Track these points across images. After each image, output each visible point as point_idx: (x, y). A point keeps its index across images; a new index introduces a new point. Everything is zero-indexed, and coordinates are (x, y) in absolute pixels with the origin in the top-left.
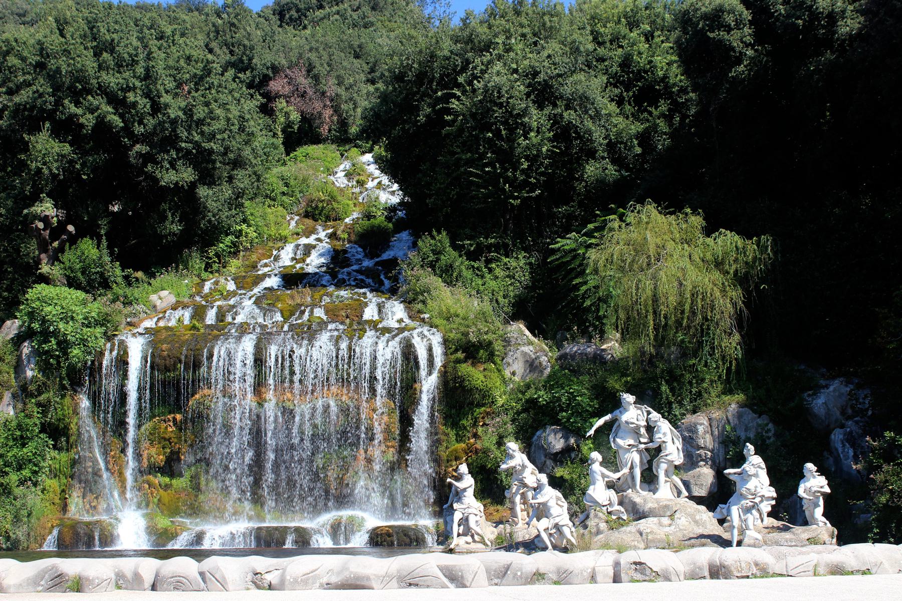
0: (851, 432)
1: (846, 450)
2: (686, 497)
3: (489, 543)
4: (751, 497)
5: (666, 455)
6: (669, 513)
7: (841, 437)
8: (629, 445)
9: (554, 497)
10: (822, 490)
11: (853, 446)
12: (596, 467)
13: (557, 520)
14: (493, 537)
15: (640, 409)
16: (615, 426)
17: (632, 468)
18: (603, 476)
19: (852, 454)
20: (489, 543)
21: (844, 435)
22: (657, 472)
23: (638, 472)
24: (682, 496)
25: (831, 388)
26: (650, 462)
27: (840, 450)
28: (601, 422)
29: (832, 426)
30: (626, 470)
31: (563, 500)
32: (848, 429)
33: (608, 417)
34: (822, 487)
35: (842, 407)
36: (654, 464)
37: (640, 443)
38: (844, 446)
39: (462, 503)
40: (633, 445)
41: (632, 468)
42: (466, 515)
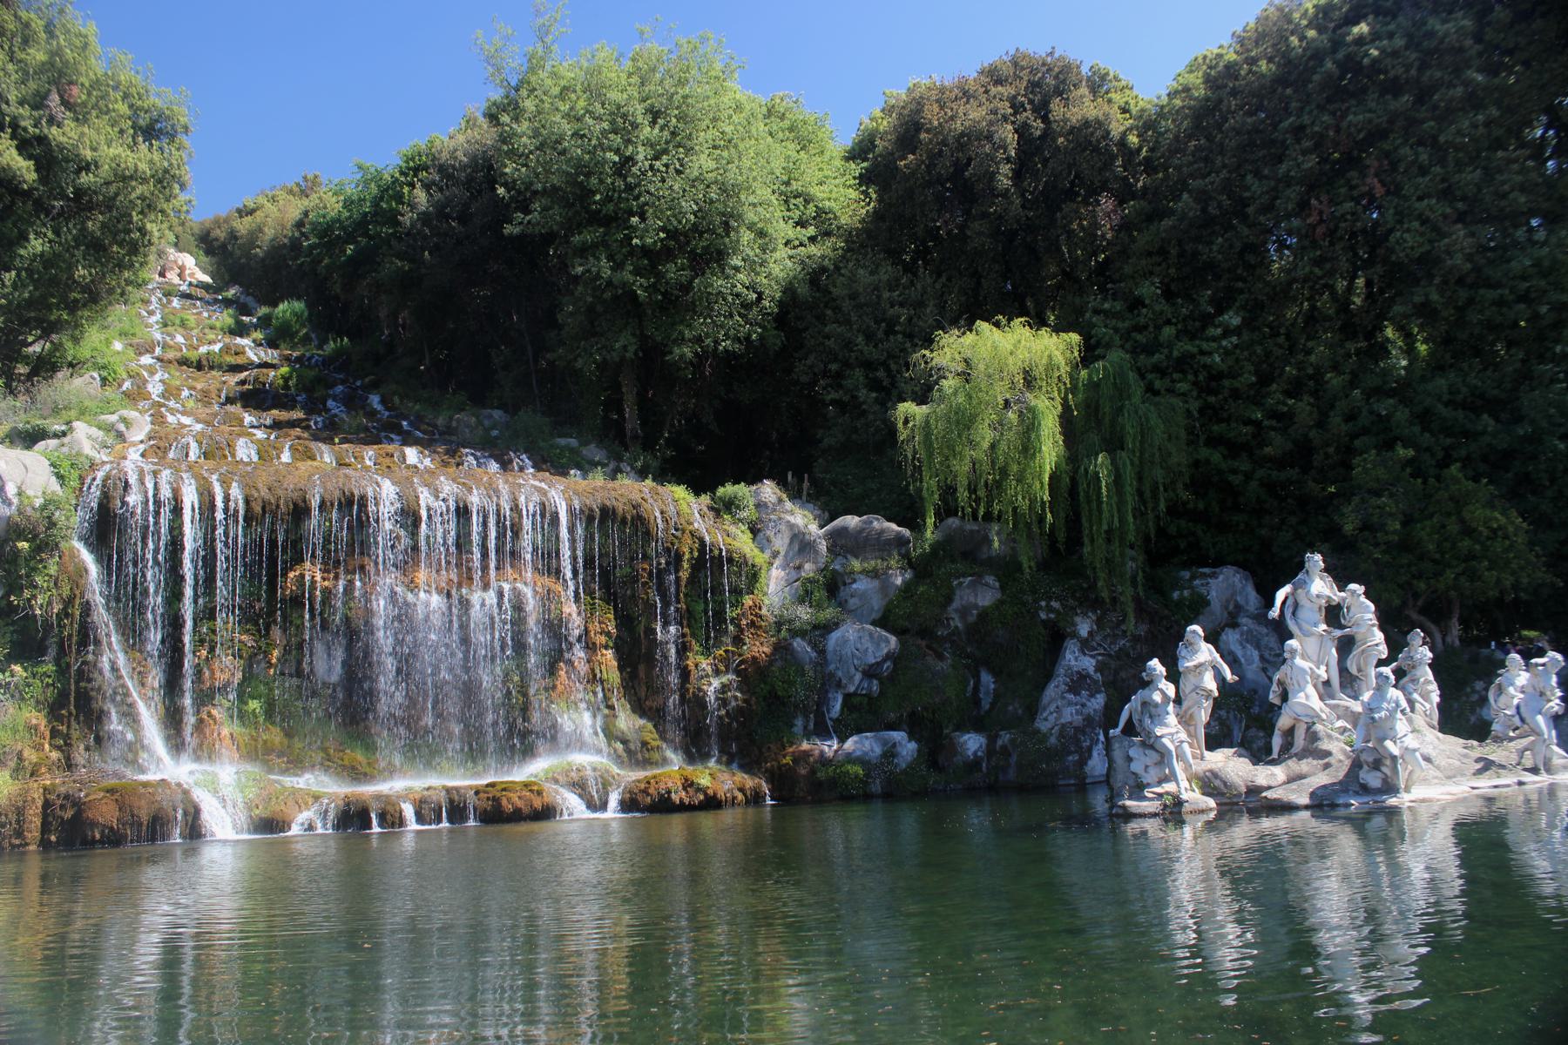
0: (1250, 631)
7: (1237, 636)
11: (1258, 647)
21: (1242, 635)
33: (1287, 589)
39: (1166, 725)
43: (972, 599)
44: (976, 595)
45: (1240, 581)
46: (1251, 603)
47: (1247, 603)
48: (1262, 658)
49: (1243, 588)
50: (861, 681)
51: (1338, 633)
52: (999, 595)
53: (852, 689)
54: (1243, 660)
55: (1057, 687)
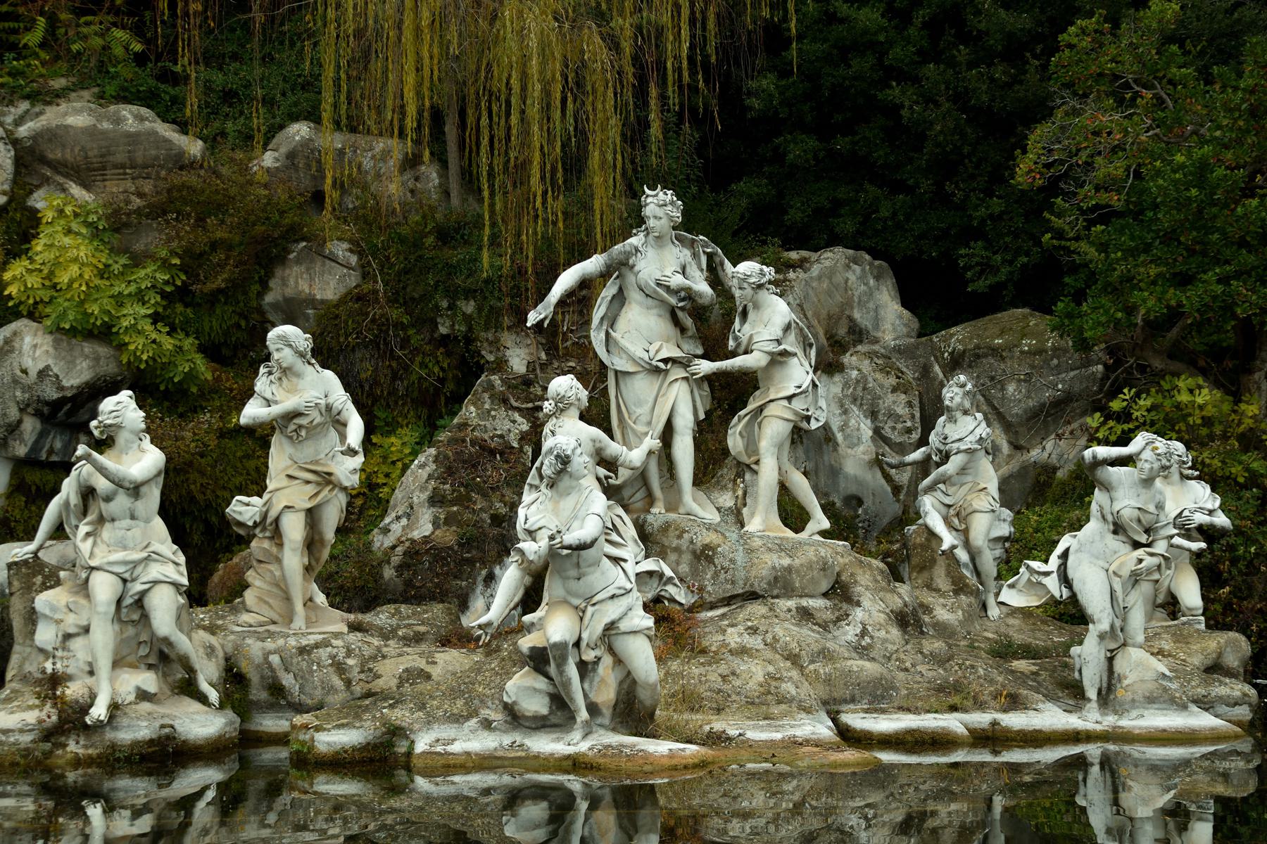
0: (862, 381)
1: (853, 422)
2: (824, 534)
5: (789, 398)
8: (665, 361)
11: (873, 414)
13: (611, 612)
15: (691, 245)
17: (668, 434)
19: (870, 433)
21: (846, 385)
24: (812, 527)
25: (815, 270)
28: (566, 280)
30: (652, 442)
32: (855, 373)
33: (592, 265)
34: (1211, 512)
35: (830, 317)
38: (845, 412)
41: (668, 434)
42: (138, 587)
43: (304, 287)
44: (312, 279)
45: (862, 278)
46: (888, 326)
47: (877, 326)
48: (877, 432)
49: (870, 294)
50: (42, 435)
51: (705, 367)
52: (353, 280)
53: (21, 451)
54: (839, 437)
55: (422, 466)
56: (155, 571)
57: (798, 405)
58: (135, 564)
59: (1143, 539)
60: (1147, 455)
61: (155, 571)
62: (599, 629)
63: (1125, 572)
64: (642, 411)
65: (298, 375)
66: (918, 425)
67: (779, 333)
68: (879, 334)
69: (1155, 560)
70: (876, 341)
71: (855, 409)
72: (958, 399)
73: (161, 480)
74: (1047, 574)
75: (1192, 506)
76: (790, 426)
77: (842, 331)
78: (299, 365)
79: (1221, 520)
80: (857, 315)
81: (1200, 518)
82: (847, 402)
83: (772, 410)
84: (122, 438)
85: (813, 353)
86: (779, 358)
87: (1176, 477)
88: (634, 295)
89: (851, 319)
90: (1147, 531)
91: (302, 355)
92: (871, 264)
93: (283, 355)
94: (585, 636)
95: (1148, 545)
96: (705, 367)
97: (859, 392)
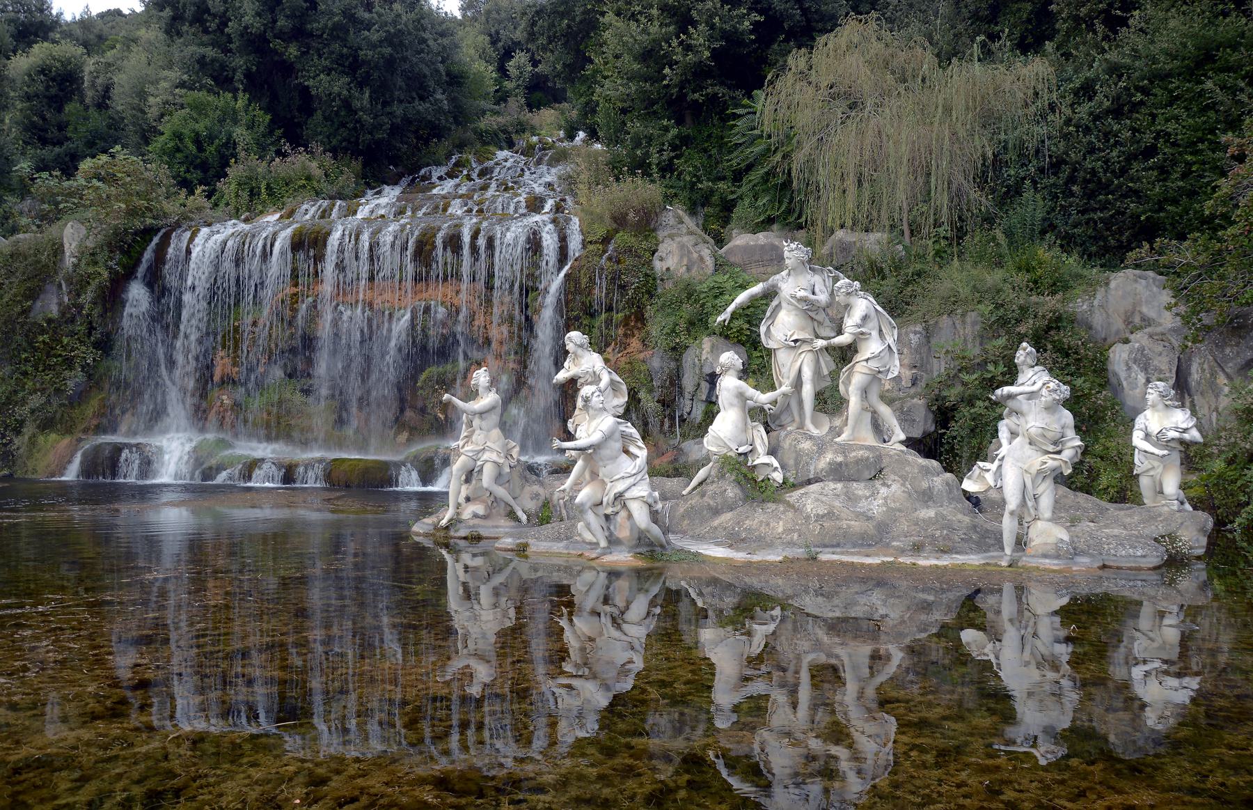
0: (1142, 349)
2: (902, 442)
3: (524, 518)
4: (1051, 448)
5: (867, 360)
6: (867, 475)
8: (796, 341)
9: (617, 435)
10: (1187, 436)
12: (729, 385)
13: (620, 487)
14: (532, 506)
16: (774, 303)
17: (798, 383)
18: (742, 397)
20: (524, 518)
22: (847, 391)
23: (808, 391)
24: (894, 439)
26: (835, 376)
27: (1123, 375)
29: (1109, 341)
30: (785, 388)
31: (640, 443)
32: (1137, 345)
34: (1185, 430)
36: (842, 377)
37: (817, 337)
38: (1129, 368)
40: (804, 341)
41: (798, 383)
42: (479, 463)
54: (1125, 383)
56: (486, 456)
57: (873, 364)
58: (479, 452)
59: (1051, 448)
60: (1044, 391)
61: (486, 456)
62: (612, 496)
63: (1034, 471)
64: (784, 370)
65: (582, 357)
66: (1174, 376)
67: (859, 321)
68: (1162, 321)
69: (1056, 464)
70: (1160, 325)
71: (1135, 367)
72: (1022, 358)
73: (499, 410)
74: (988, 471)
75: (1168, 426)
76: (869, 378)
77: (1137, 320)
78: (580, 351)
79: (1195, 435)
80: (1145, 310)
81: (1173, 434)
82: (1131, 364)
83: (858, 368)
84: (480, 390)
85: (896, 332)
86: (860, 337)
87: (1161, 406)
88: (784, 305)
89: (1140, 312)
90: (1055, 443)
91: (581, 346)
92: (1154, 279)
93: (570, 347)
94: (605, 500)
95: (1059, 452)
96: (820, 343)
97: (1139, 356)
